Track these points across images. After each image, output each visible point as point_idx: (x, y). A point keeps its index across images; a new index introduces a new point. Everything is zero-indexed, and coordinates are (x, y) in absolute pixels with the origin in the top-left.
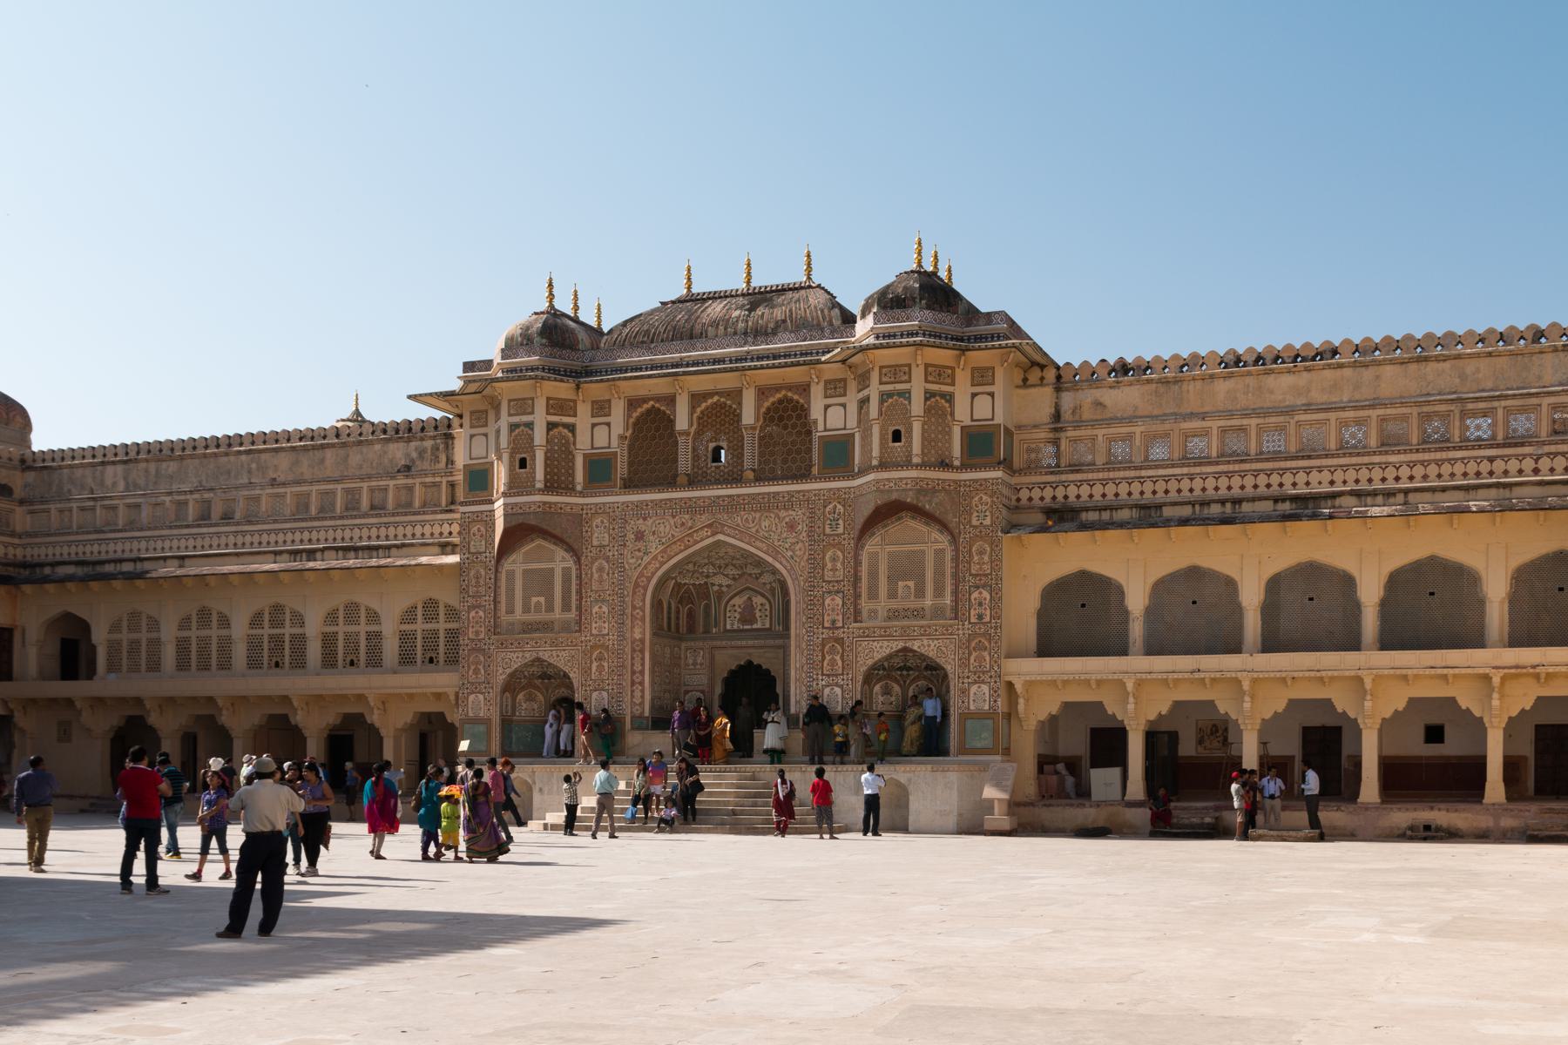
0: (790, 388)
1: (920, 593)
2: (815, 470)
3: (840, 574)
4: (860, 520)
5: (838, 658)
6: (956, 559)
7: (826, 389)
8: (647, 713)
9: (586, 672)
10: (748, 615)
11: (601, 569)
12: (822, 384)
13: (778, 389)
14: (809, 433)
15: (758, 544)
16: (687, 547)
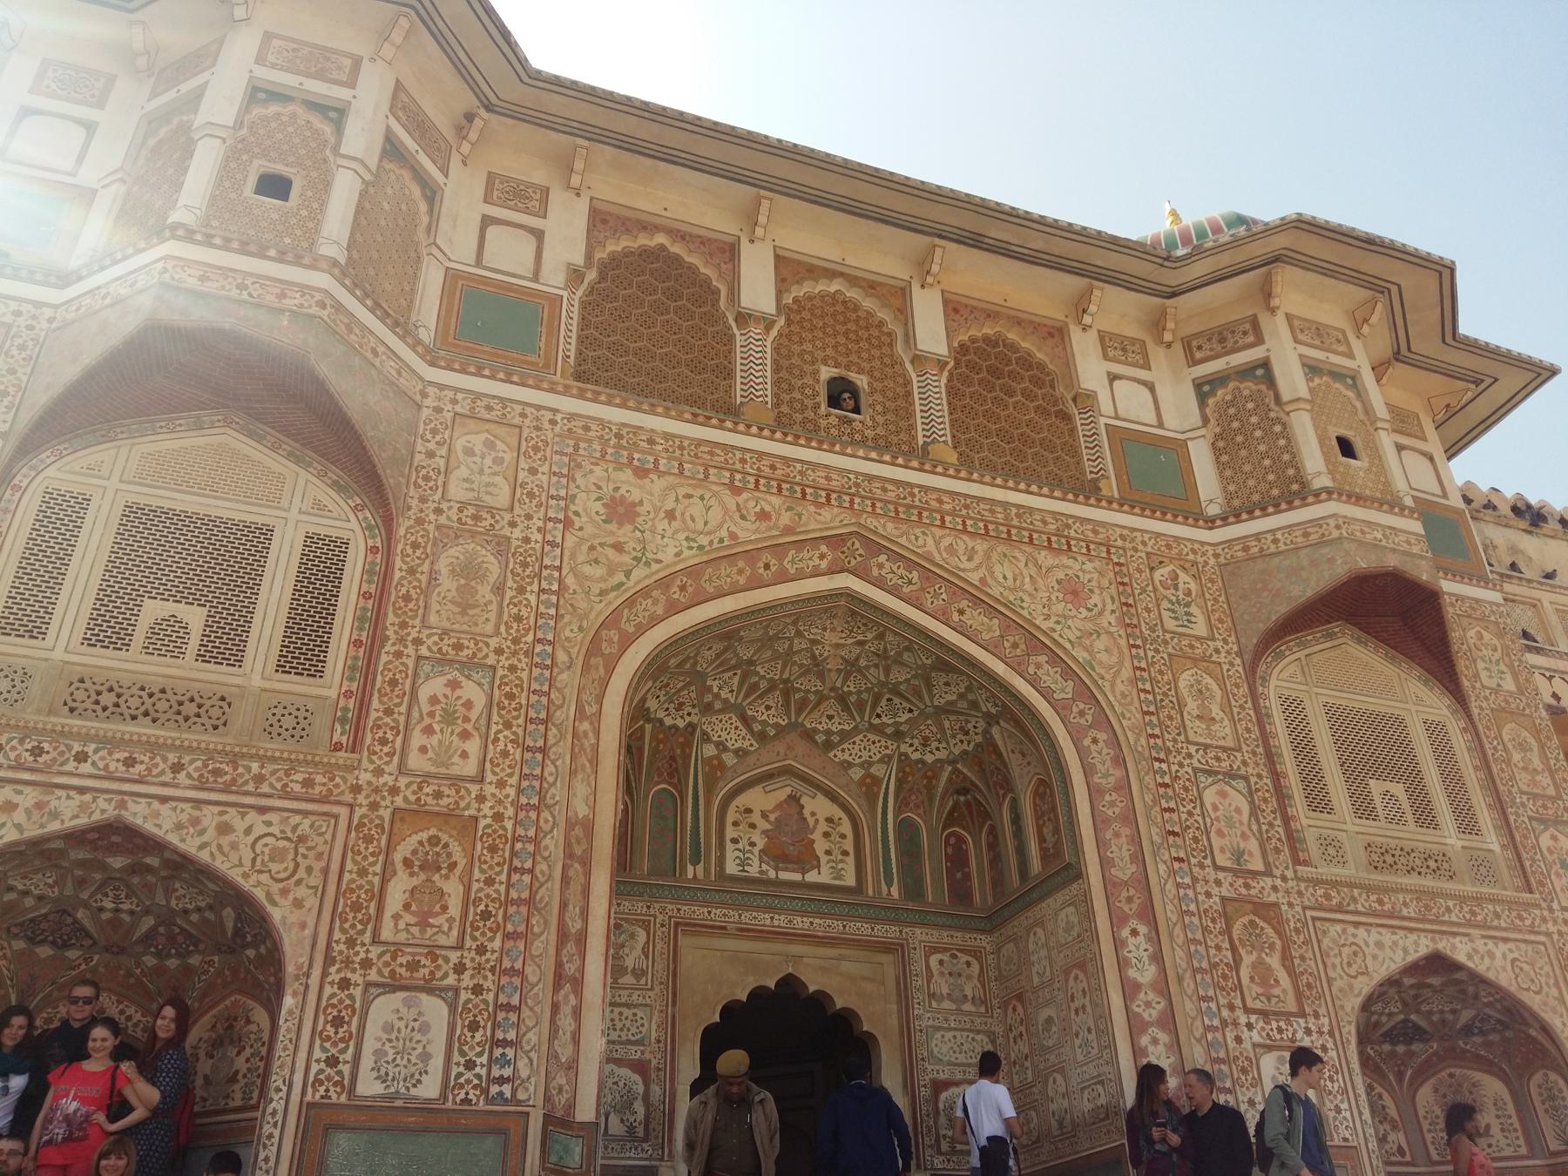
0: (1017, 322)
1: (1425, 816)
2: (1111, 487)
3: (1224, 732)
4: (1282, 609)
5: (1274, 961)
6: (1478, 746)
7: (1104, 348)
8: (586, 1112)
9: (359, 908)
10: (791, 847)
11: (468, 571)
12: (1092, 335)
13: (991, 315)
14: (1066, 417)
15: (974, 618)
16: (756, 584)
